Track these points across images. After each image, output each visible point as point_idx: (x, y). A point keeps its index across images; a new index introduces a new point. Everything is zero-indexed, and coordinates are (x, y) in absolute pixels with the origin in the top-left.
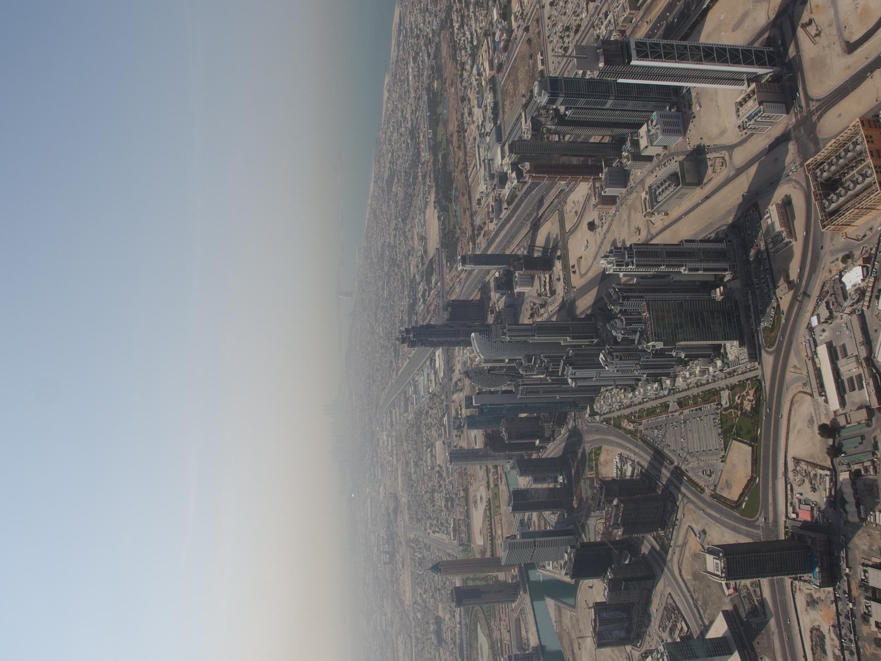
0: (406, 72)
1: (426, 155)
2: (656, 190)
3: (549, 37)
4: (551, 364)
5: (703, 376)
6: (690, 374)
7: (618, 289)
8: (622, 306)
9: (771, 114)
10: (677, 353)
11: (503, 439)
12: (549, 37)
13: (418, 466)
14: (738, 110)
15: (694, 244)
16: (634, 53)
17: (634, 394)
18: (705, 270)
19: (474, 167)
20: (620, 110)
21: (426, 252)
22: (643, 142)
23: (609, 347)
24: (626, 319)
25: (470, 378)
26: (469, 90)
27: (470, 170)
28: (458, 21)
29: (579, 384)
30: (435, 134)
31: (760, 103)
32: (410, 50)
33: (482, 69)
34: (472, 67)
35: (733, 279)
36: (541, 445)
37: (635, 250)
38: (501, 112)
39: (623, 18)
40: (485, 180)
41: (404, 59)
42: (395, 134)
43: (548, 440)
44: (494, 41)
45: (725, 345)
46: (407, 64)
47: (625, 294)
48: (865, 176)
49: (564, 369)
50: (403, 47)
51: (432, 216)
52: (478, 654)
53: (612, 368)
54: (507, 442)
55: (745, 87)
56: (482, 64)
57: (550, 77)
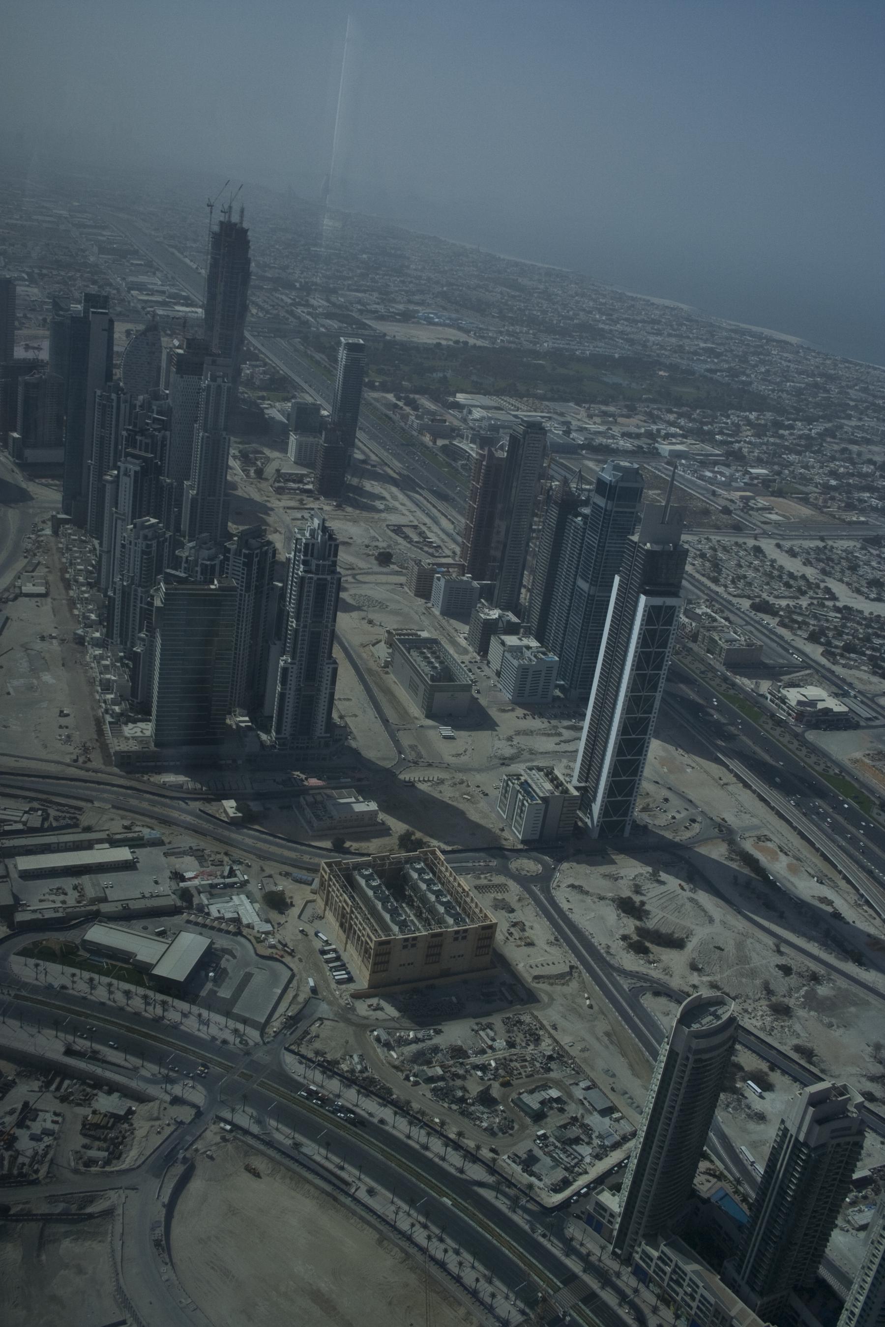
0: (691, 336)
1: (547, 344)
2: (429, 648)
3: (707, 539)
4: (149, 441)
5: (101, 685)
6: (106, 666)
8: (235, 554)
9: (525, 816)
10: (142, 640)
12: (707, 539)
14: (540, 769)
15: (329, 682)
16: (658, 601)
17: (83, 585)
18: (282, 696)
20: (570, 607)
21: (382, 318)
22: (512, 640)
23: (167, 536)
24: (213, 567)
25: (144, 333)
26: (643, 418)
27: (512, 401)
28: (758, 418)
29: (108, 487)
31: (545, 800)
32: (727, 347)
34: (681, 428)
35: (262, 744)
36: (11, 442)
37: (329, 578)
38: (600, 457)
39: (717, 638)
40: (490, 418)
42: (591, 304)
43: (18, 454)
44: (716, 463)
45: (150, 721)
46: (705, 341)
47: (256, 560)
48: (403, 925)
49: (134, 456)
50: (732, 338)
51: (448, 336)
53: (129, 537)
54: (20, 379)
55: (575, 781)
57: (642, 488)
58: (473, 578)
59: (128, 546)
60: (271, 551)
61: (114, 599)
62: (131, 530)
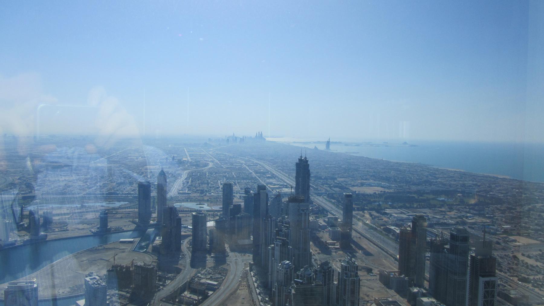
1: (414, 188)
4: (284, 233)
7: (331, 270)
11: (238, 214)
13: (223, 177)
19: (407, 212)
21: (354, 186)
26: (456, 211)
30: (427, 193)
33: (470, 219)
34: (472, 214)
37: (355, 279)
41: (475, 179)
42: (427, 173)
46: (473, 181)
47: (327, 274)
51: (378, 190)
52: (110, 202)
56: (474, 219)
58: (405, 276)
59: (279, 272)
60: (332, 270)
61: (275, 292)
62: (280, 266)
